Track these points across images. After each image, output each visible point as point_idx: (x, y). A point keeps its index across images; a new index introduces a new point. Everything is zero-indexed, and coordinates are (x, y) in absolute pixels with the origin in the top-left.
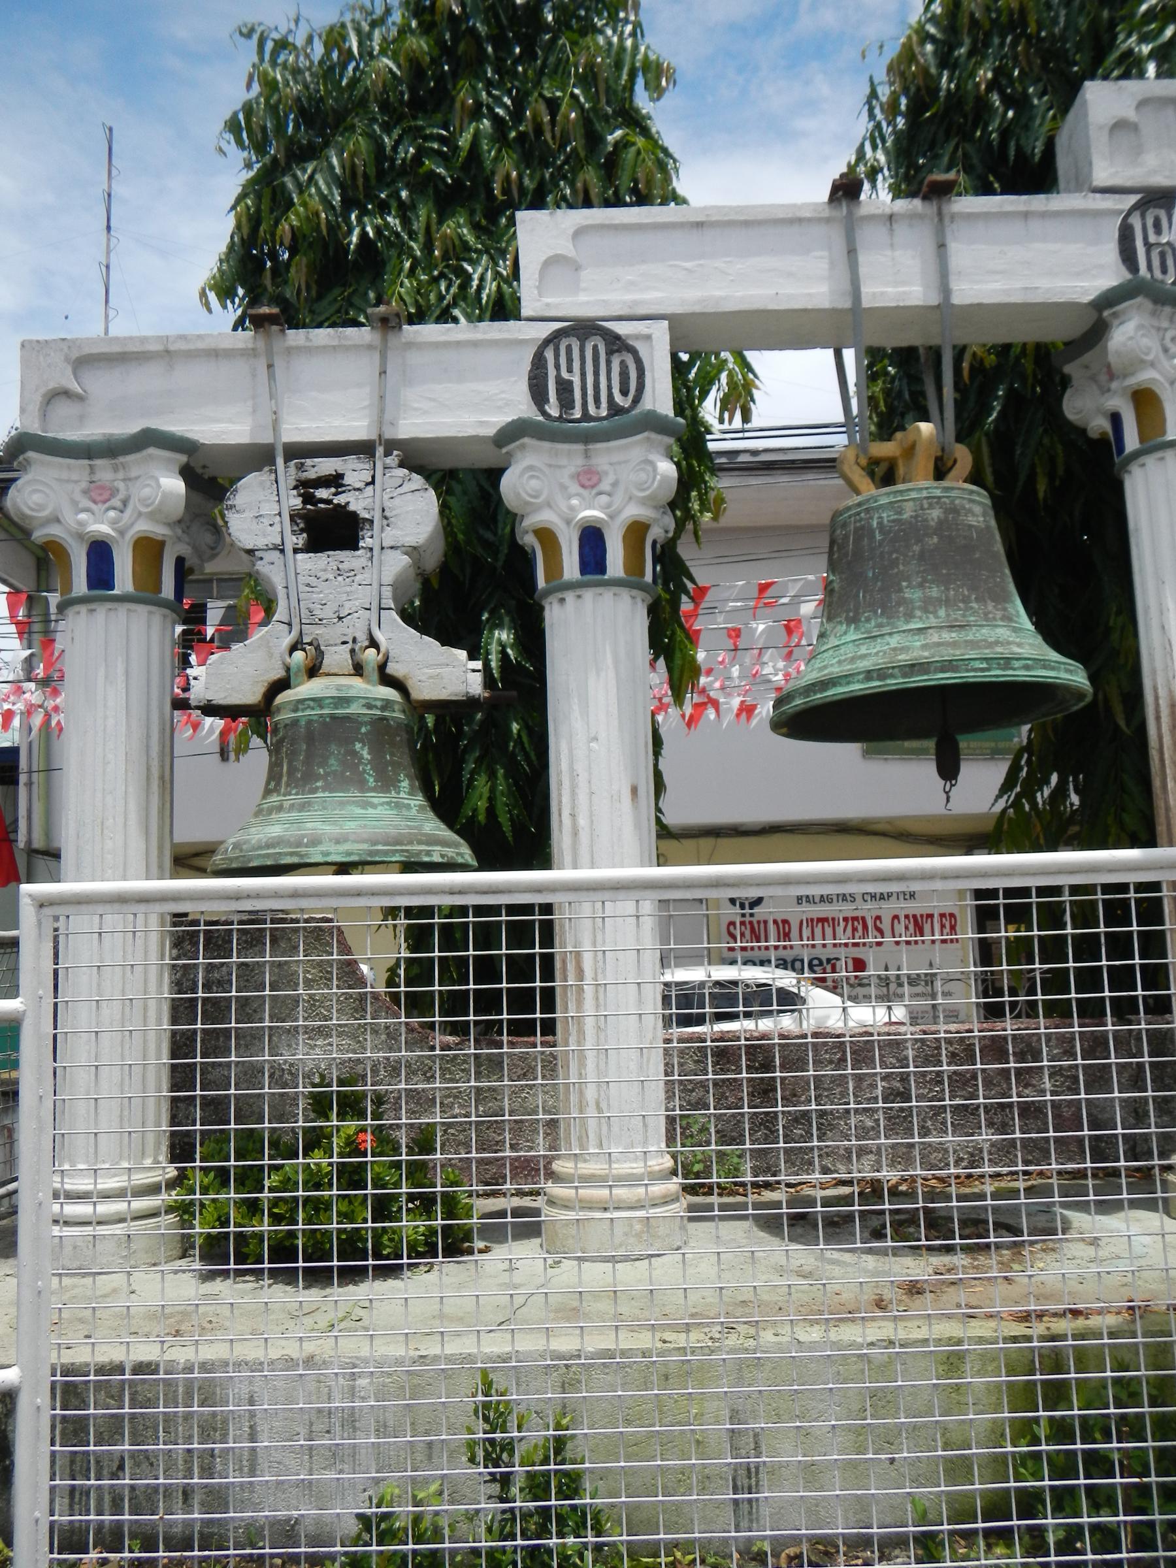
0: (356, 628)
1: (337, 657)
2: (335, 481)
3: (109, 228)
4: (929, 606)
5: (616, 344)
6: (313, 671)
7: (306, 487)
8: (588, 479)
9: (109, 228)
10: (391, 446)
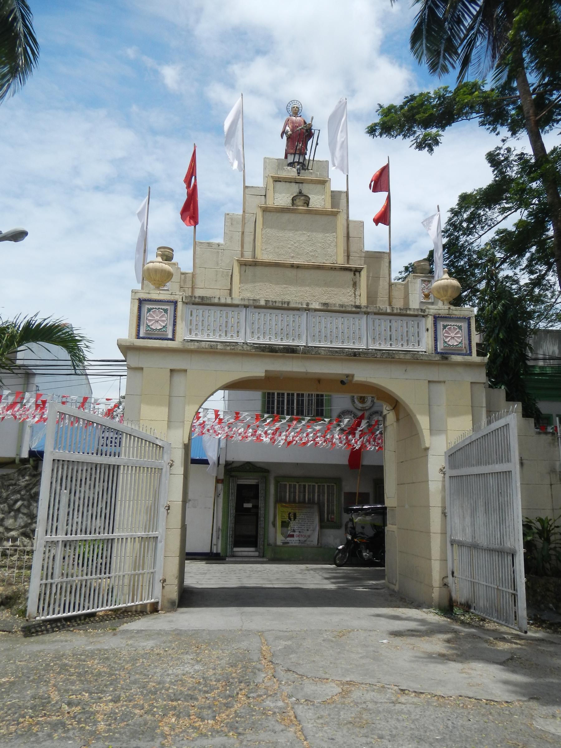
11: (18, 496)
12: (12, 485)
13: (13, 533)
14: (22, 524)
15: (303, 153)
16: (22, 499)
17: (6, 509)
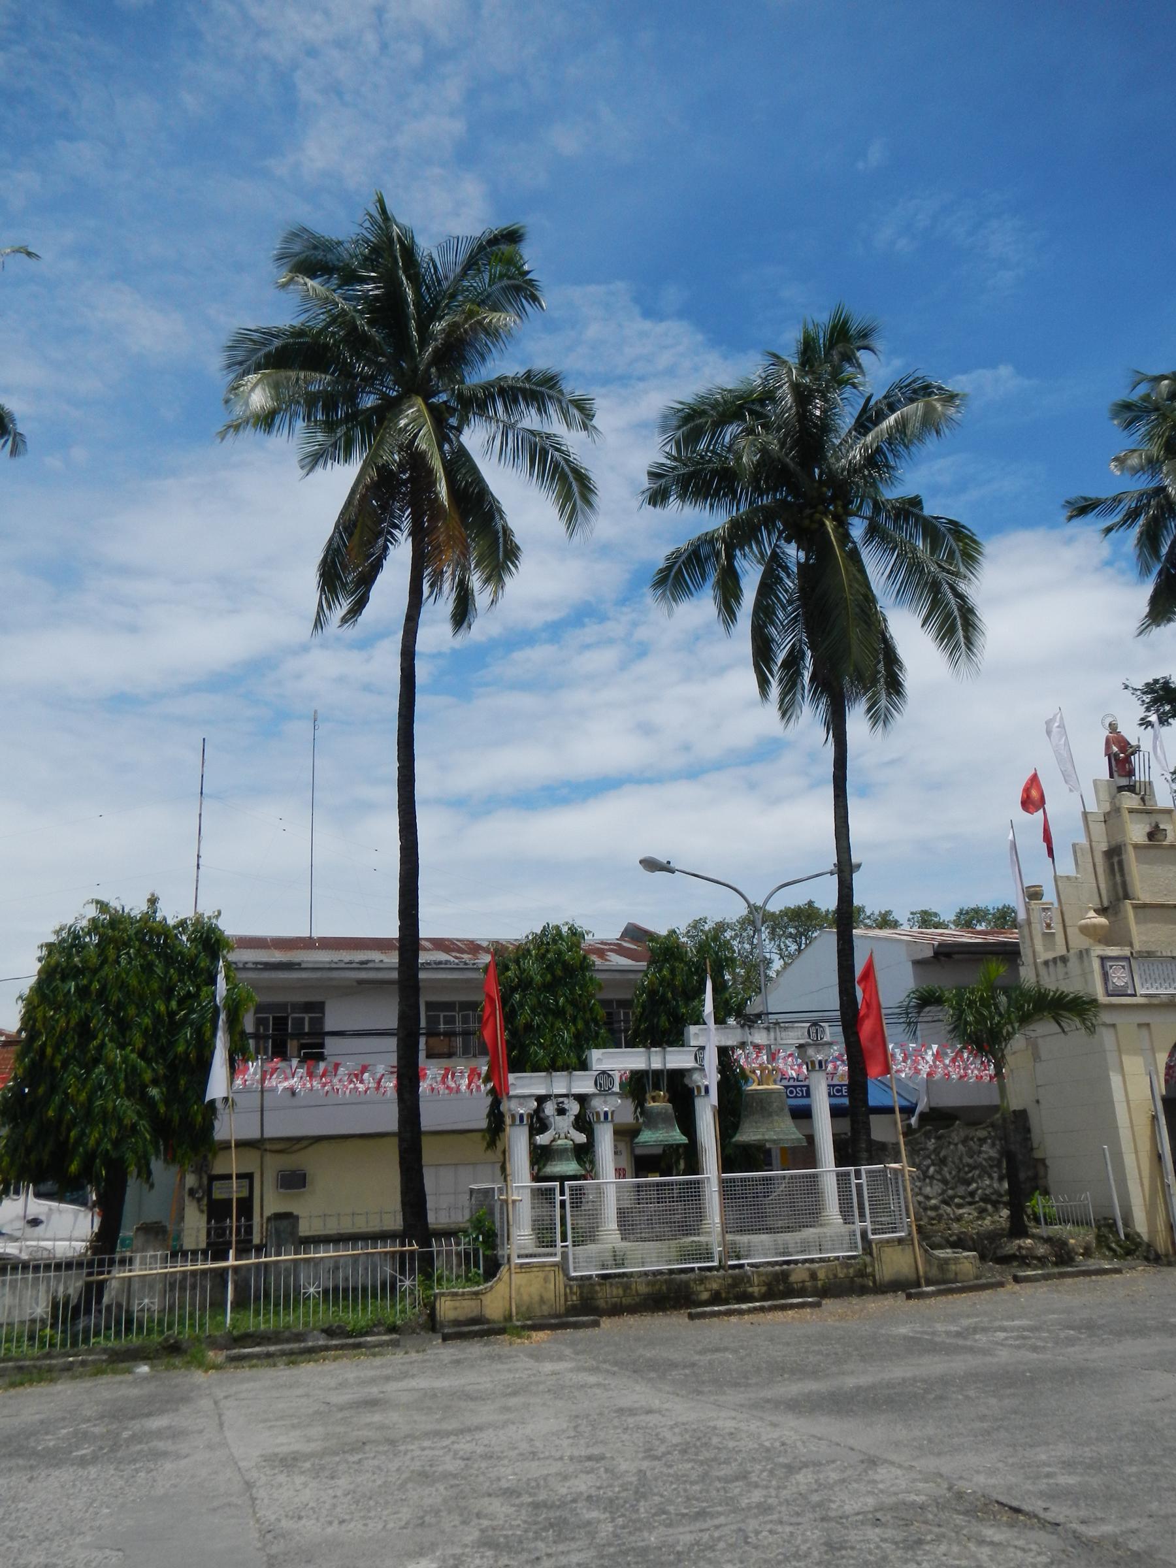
0: (566, 1130)
1: (562, 1135)
2: (562, 1103)
3: (202, 793)
4: (663, 1128)
5: (609, 1076)
6: (559, 1138)
7: (558, 1104)
8: (605, 1102)
9: (202, 793)
10: (573, 1095)
11: (928, 1162)
12: (922, 1149)
13: (933, 1202)
14: (940, 1191)
15: (1131, 773)
16: (933, 1164)
17: (921, 1176)
